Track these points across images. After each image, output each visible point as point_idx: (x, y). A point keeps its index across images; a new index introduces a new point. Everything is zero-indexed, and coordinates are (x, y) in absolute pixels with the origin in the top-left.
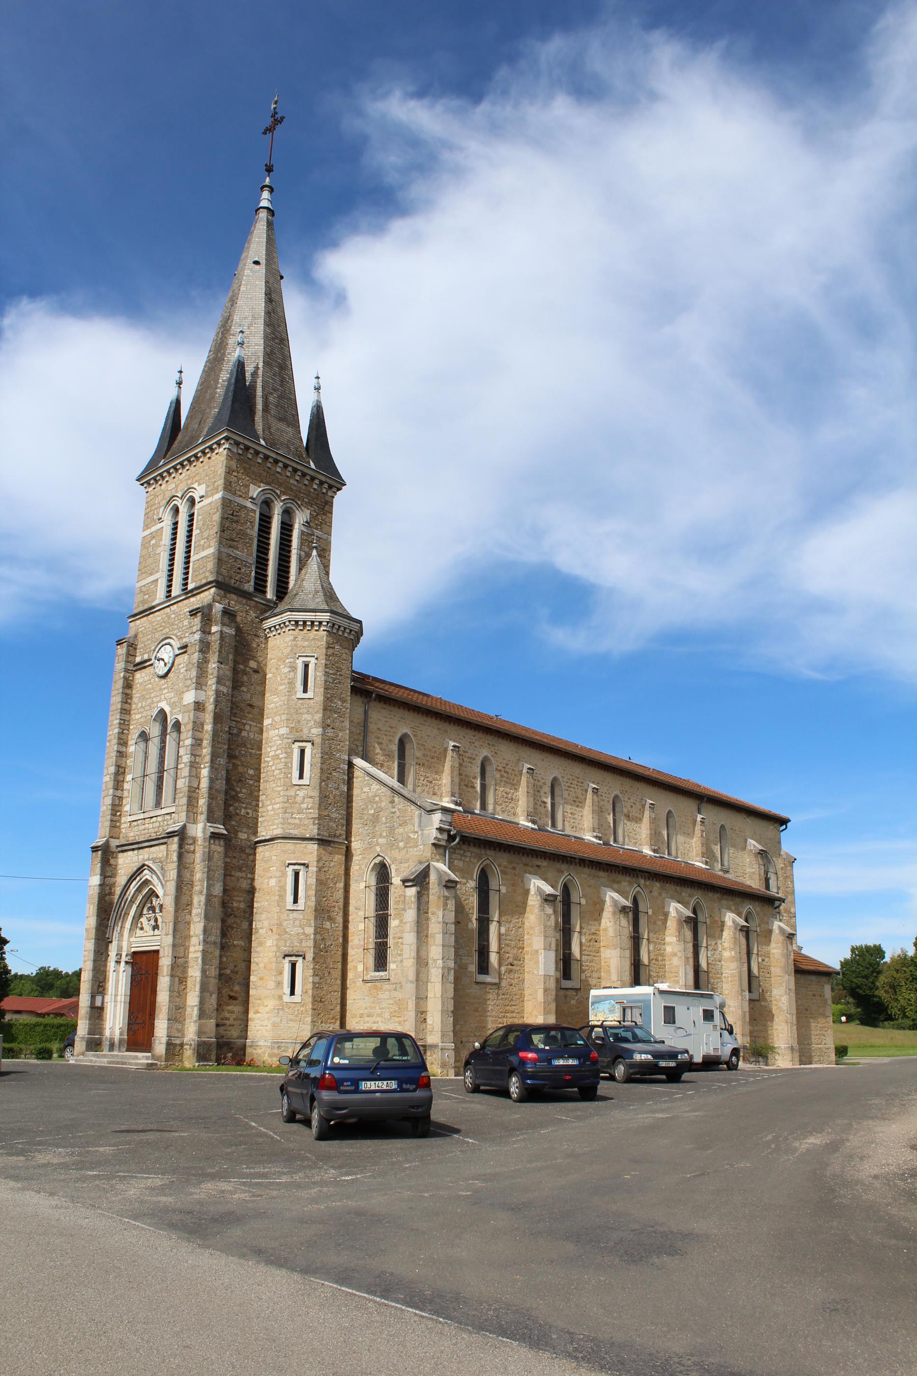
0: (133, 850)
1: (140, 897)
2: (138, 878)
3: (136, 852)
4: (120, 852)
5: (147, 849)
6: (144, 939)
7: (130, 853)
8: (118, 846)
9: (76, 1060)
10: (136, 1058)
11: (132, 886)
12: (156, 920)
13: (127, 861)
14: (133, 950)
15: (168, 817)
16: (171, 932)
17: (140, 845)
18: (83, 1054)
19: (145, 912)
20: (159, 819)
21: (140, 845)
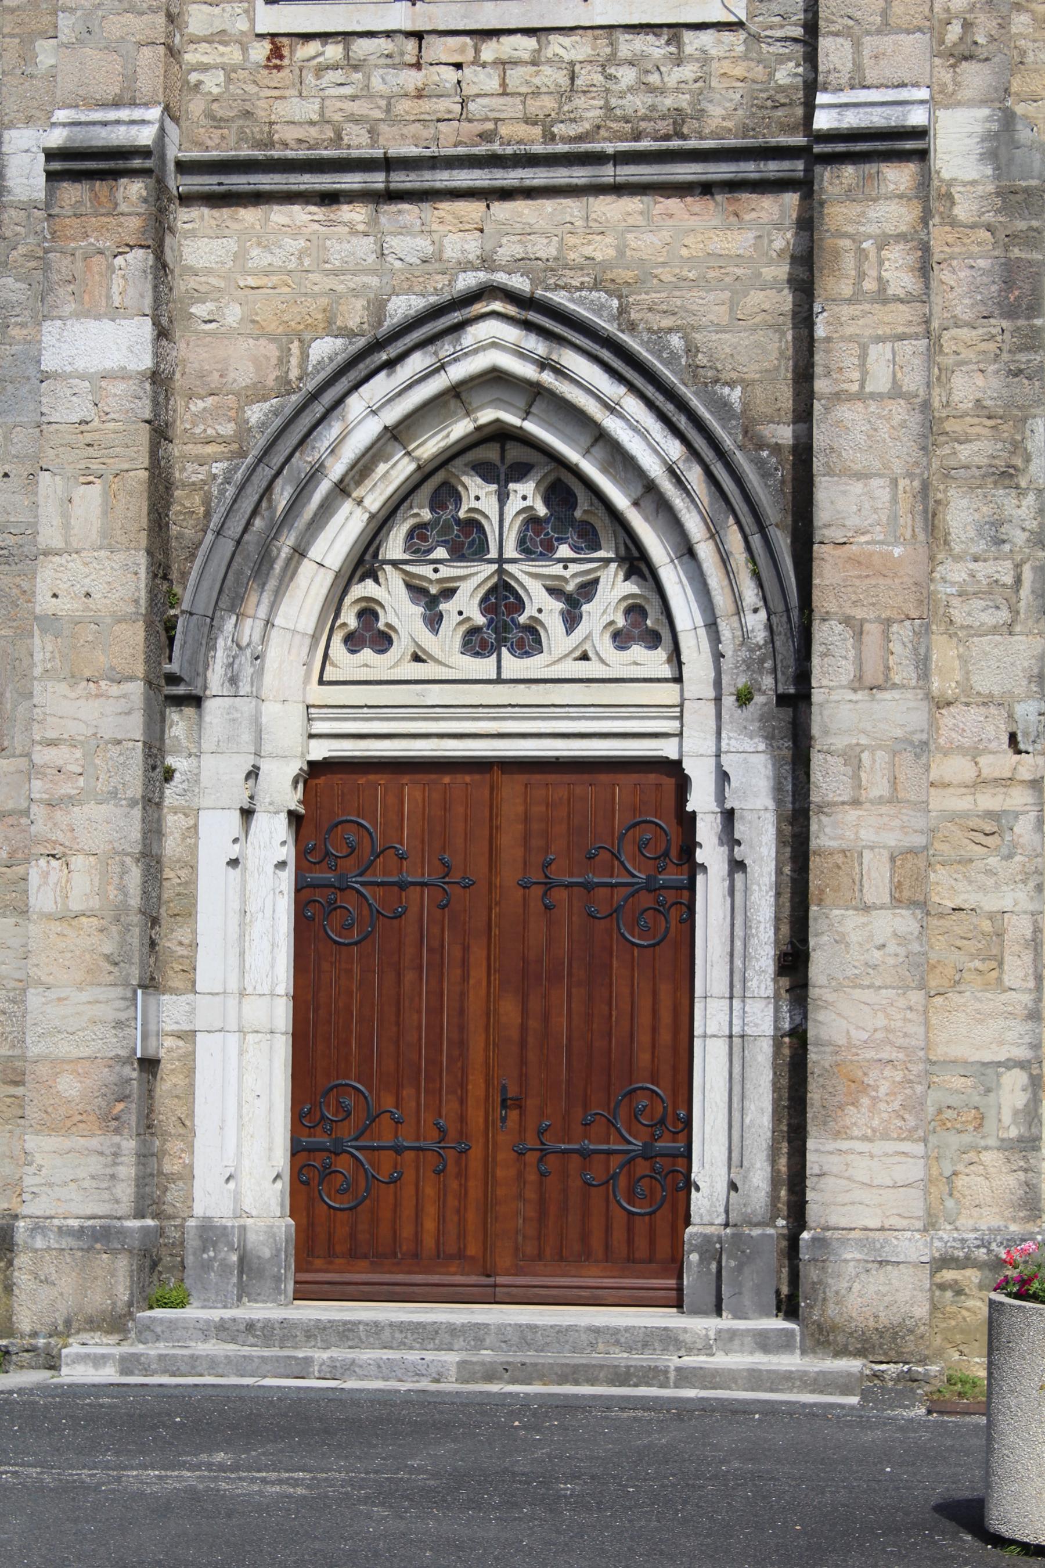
0: (330, 198)
1: (397, 470)
2: (417, 362)
3: (355, 214)
4: (186, 199)
5: (473, 209)
6: (435, 694)
7: (300, 214)
8: (184, 167)
9: (127, 1365)
10: (670, 1340)
11: (356, 404)
12: (502, 598)
13: (258, 257)
14: (319, 751)
15: (654, 47)
16: (904, 672)
17: (402, 180)
18: (116, 1323)
19: (394, 547)
20: (556, 45)
21: (402, 180)
